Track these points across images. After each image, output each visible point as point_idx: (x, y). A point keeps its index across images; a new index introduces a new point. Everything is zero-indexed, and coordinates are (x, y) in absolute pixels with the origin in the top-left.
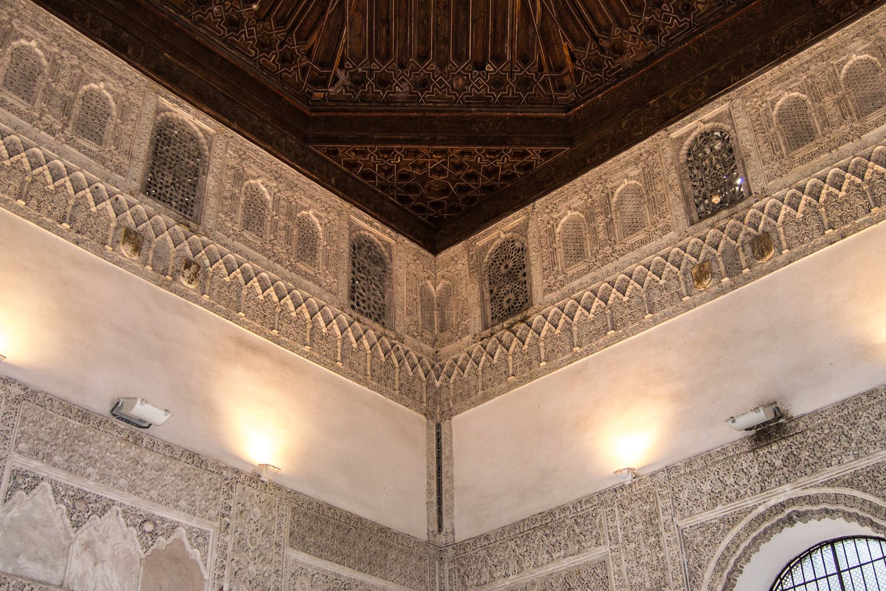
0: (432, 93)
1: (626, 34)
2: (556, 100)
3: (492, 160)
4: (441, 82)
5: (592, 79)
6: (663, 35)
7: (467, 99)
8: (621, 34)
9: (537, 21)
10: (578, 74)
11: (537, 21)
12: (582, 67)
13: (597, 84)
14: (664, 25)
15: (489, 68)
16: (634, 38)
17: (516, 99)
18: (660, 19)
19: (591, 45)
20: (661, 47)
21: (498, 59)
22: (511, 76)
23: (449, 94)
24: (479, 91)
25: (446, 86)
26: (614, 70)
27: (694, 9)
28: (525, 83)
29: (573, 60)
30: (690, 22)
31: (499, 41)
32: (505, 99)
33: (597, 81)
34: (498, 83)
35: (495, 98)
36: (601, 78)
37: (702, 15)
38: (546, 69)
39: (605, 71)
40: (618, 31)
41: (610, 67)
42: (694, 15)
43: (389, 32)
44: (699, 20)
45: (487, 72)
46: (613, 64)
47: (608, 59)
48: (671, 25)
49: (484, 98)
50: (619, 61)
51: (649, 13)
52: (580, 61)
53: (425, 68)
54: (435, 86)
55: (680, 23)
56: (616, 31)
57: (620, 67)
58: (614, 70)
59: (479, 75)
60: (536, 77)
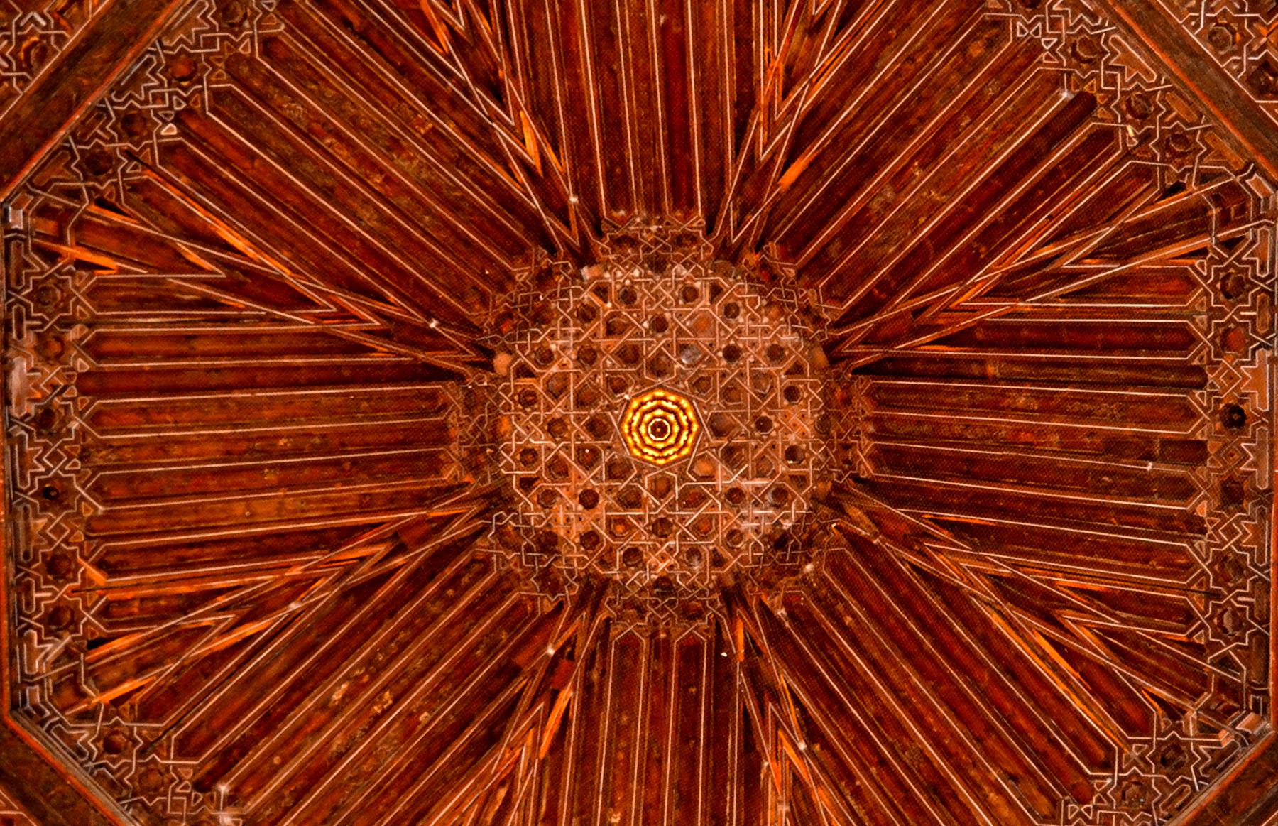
0: (204, 17)
1: (70, 377)
2: (30, 193)
3: (21, 39)
4: (210, 43)
5: (28, 275)
6: (31, 438)
7: (149, 62)
8: (73, 369)
9: (182, 245)
10: (52, 257)
11: (182, 245)
12: (58, 271)
13: (13, 277)
14: (46, 447)
15: (171, 129)
16: (54, 387)
17: (84, 135)
18: (60, 447)
19: (86, 308)
20: (12, 424)
21: (169, 150)
22: (129, 155)
23: (181, 41)
24: (147, 89)
25: (197, 46)
26: (20, 321)
27: (44, 509)
28: (97, 164)
29: (80, 264)
30: (25, 492)
31: (195, 169)
32: (99, 117)
33: (18, 281)
34: (132, 124)
35: (113, 103)
36: (19, 292)
37: (26, 518)
38: (94, 209)
39: (27, 307)
40: (82, 366)
41: (29, 318)
42: (34, 505)
43: (346, 24)
44: (20, 509)
45: (165, 123)
46: (31, 328)
47: (45, 322)
48: (39, 459)
49: (127, 86)
50: (29, 339)
51: (82, 433)
52: (70, 273)
53: (252, 37)
54: (213, 29)
55: (33, 475)
56: (83, 364)
57: (20, 335)
58: (20, 321)
59: (171, 107)
60: (94, 188)
